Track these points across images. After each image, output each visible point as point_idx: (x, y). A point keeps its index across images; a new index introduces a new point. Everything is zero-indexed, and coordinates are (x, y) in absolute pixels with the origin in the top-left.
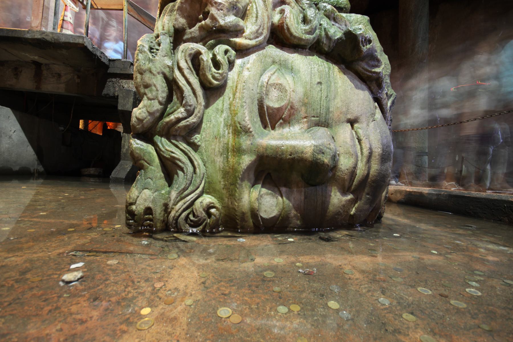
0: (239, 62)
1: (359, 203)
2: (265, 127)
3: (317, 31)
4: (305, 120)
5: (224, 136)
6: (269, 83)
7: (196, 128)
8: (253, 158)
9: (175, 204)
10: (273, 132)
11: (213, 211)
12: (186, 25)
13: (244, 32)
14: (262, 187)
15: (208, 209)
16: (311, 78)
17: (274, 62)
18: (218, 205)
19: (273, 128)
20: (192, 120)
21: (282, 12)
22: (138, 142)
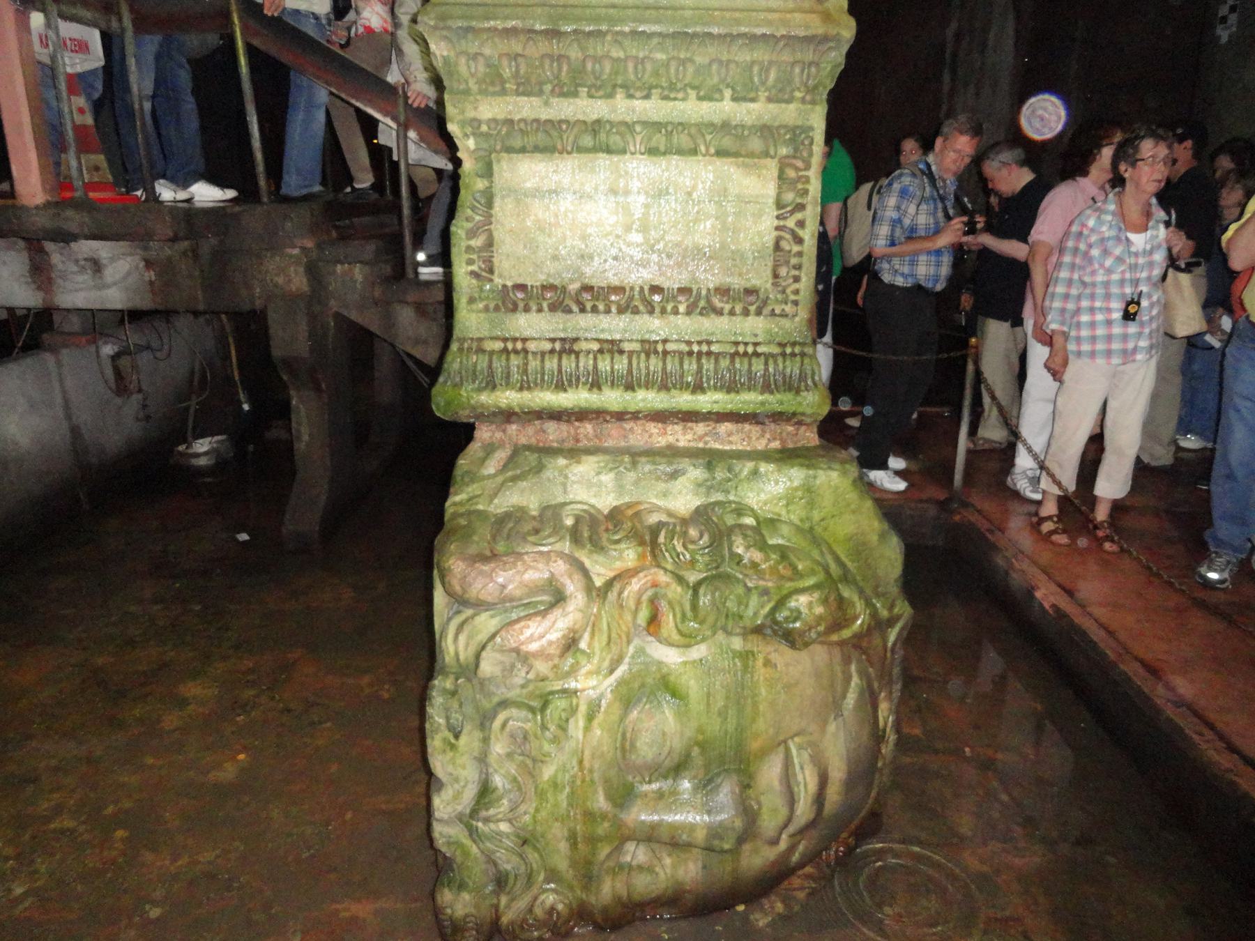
5: (568, 816)
9: (508, 906)
16: (708, 704)
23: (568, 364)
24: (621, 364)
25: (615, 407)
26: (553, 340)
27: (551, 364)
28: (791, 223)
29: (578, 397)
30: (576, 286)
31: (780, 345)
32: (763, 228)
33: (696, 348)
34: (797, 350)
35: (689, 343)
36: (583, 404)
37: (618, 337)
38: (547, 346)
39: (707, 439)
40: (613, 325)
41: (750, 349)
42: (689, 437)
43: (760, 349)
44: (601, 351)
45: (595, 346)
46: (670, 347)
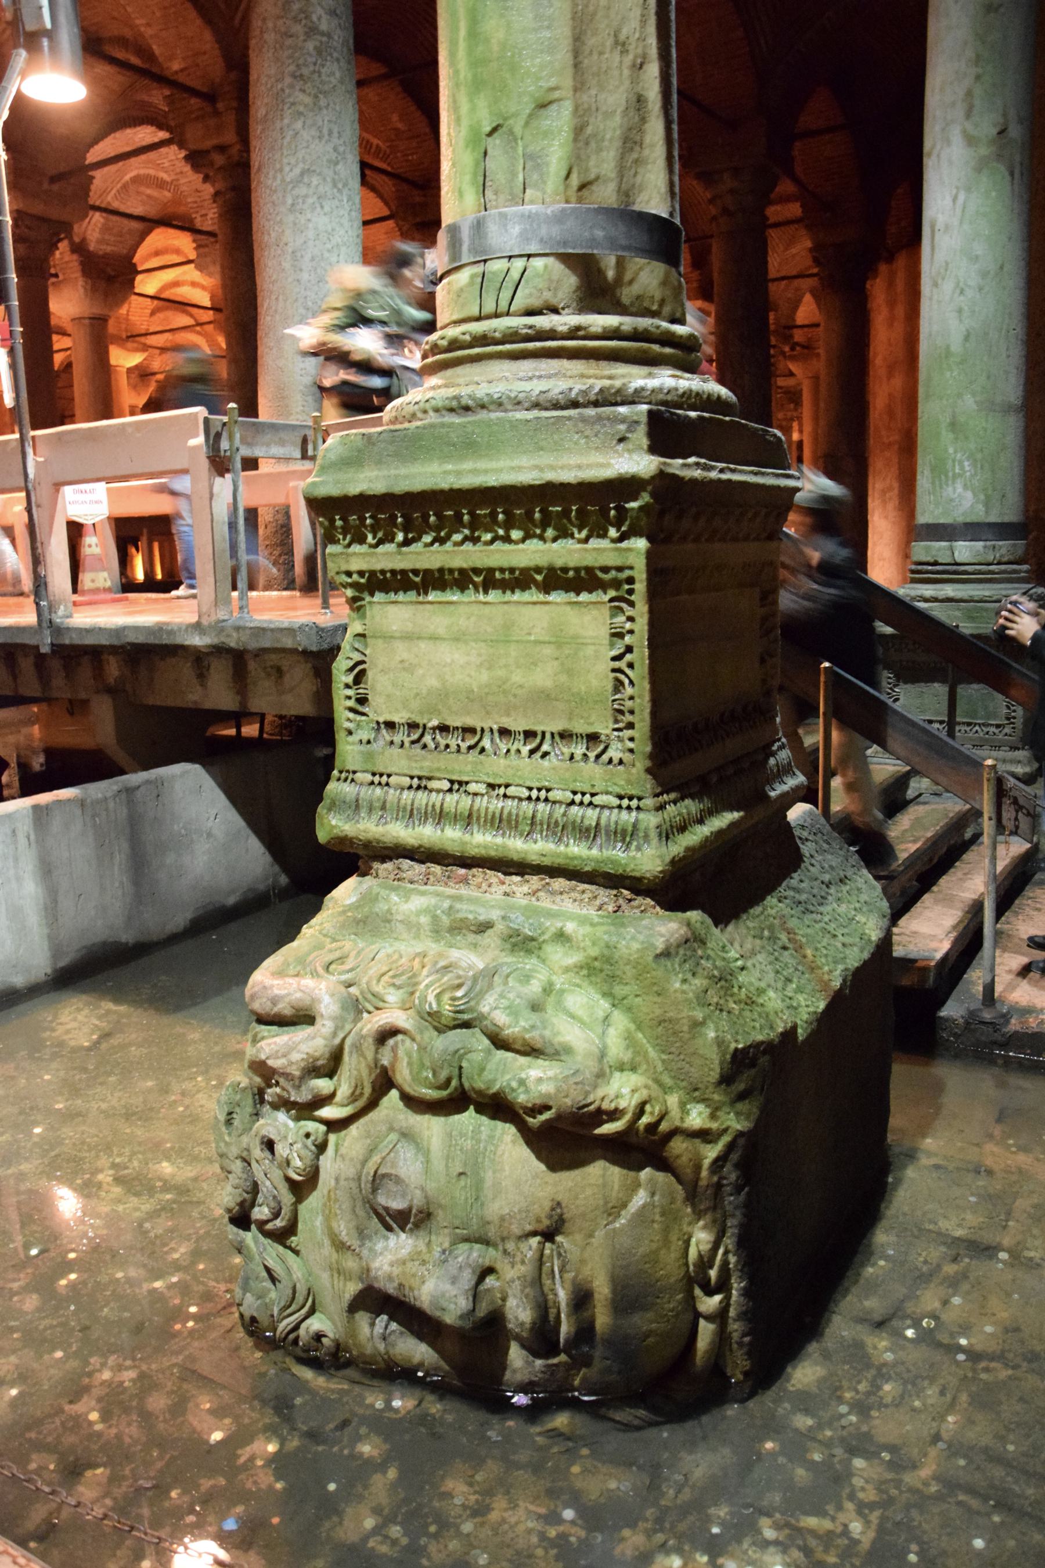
0: (332, 1138)
1: (584, 1371)
2: (389, 1229)
3: (454, 1083)
4: (446, 1231)
6: (379, 1172)
7: (291, 1229)
8: (360, 1286)
10: (403, 1236)
11: (324, 1340)
12: (263, 1085)
13: (333, 1095)
14: (392, 1318)
15: (319, 1337)
16: (447, 1166)
17: (391, 1129)
18: (331, 1335)
19: (403, 1230)
20: (279, 1223)
21: (394, 1049)
22: (235, 1229)
23: (421, 797)
24: (466, 802)
25: (454, 849)
26: (412, 778)
27: (407, 796)
28: (622, 664)
29: (427, 834)
30: (435, 723)
31: (621, 797)
32: (598, 673)
33: (534, 794)
34: (634, 803)
35: (530, 789)
36: (426, 842)
37: (465, 779)
38: (406, 781)
39: (541, 894)
40: (463, 766)
41: (587, 799)
42: (525, 889)
43: (597, 800)
44: (450, 790)
45: (446, 785)
46: (511, 791)
